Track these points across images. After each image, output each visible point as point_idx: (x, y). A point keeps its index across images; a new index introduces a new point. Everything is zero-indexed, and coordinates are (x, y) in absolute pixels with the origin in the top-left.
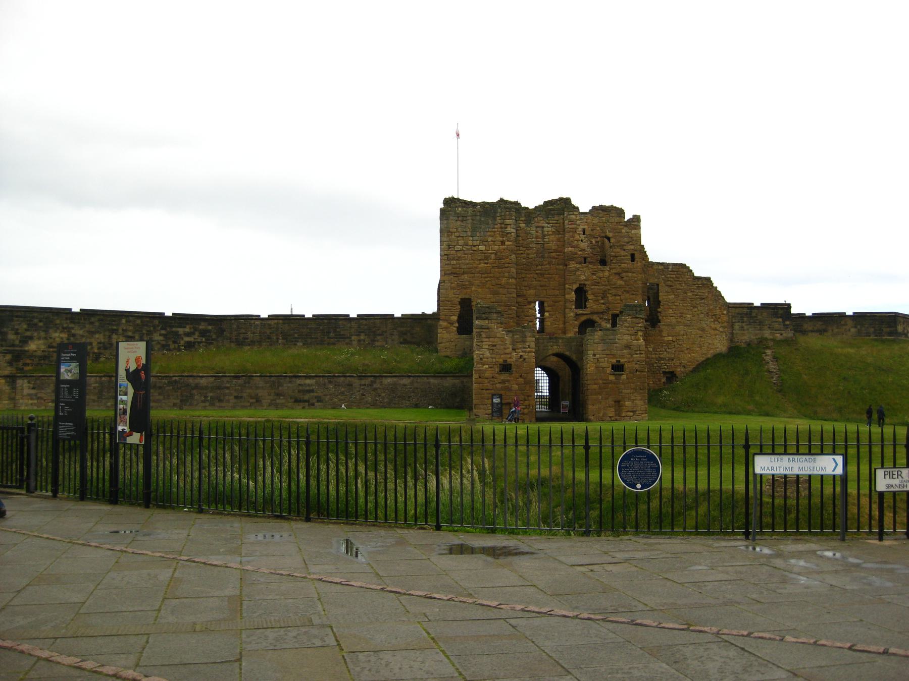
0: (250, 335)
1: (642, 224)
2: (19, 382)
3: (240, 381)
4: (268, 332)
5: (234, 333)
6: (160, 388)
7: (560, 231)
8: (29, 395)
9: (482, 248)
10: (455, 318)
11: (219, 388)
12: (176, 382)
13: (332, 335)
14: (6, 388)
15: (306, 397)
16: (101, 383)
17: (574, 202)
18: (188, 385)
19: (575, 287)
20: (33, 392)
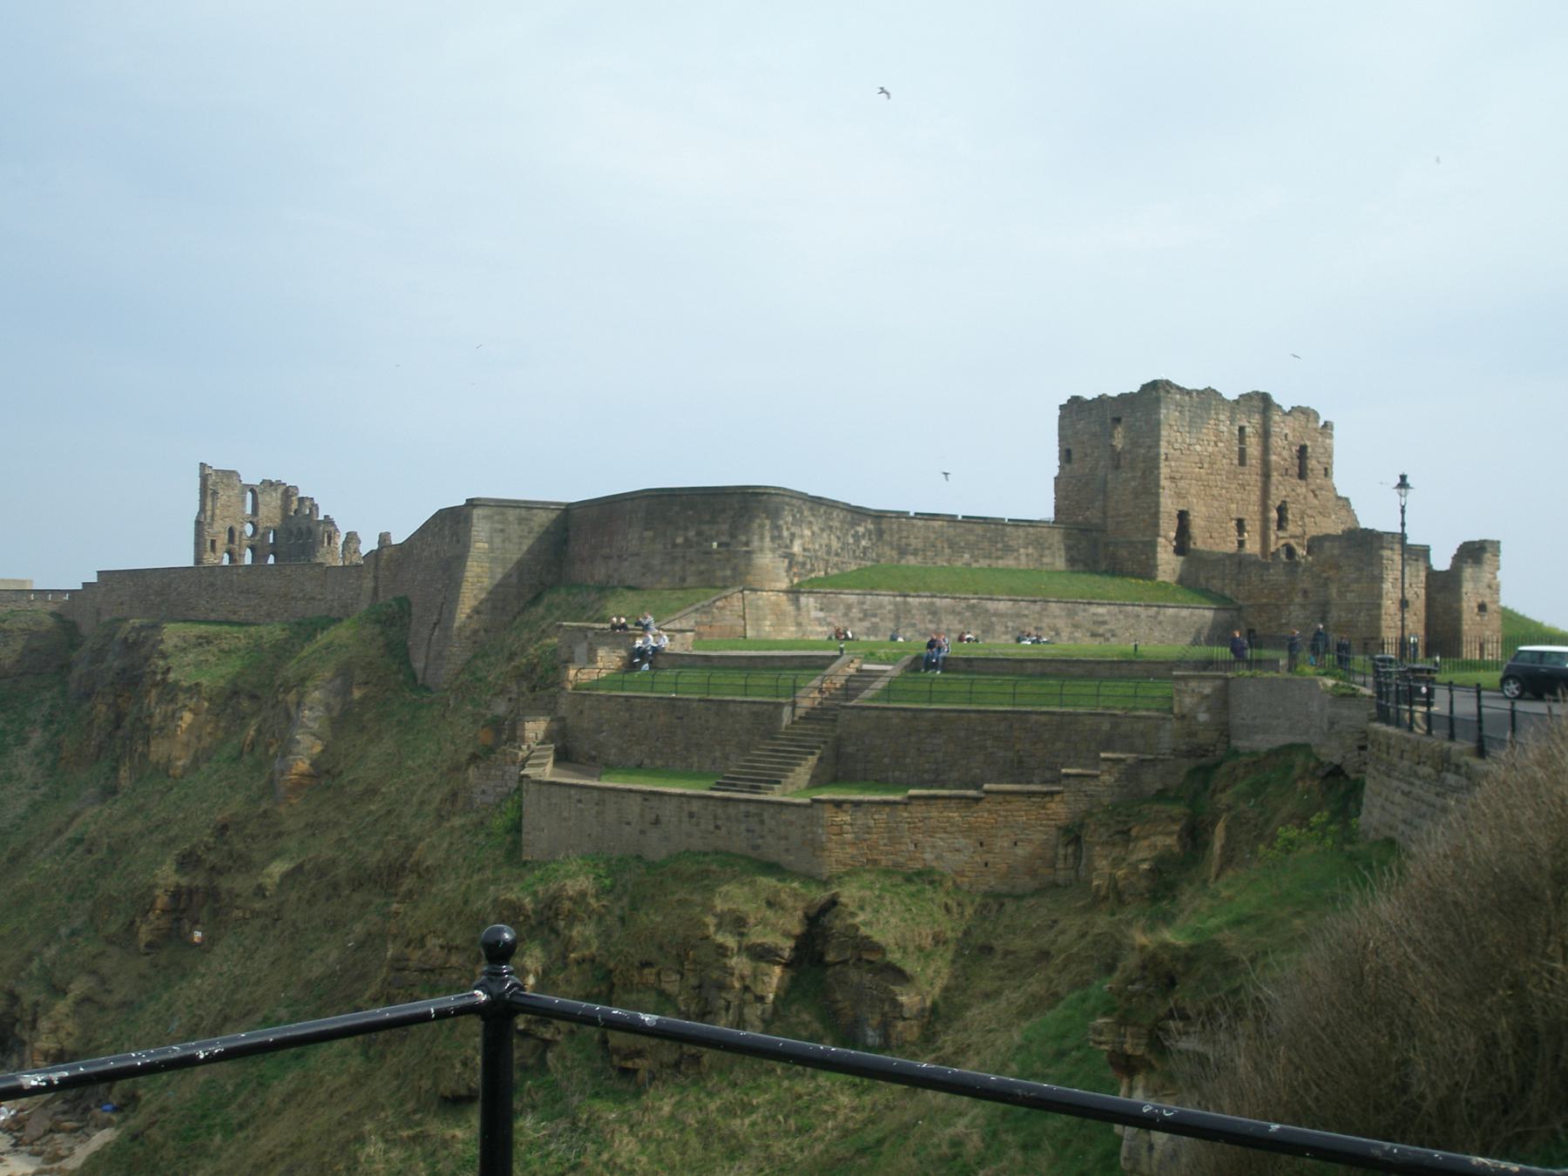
0: (913, 541)
1: (1335, 433)
2: (803, 599)
3: (1037, 607)
4: (933, 536)
5: (896, 537)
6: (959, 613)
7: (1265, 435)
8: (818, 619)
9: (1198, 448)
10: (1173, 535)
11: (1018, 615)
12: (974, 606)
13: (1000, 546)
14: (790, 609)
15: (1101, 631)
16: (896, 604)
17: (1276, 399)
18: (987, 611)
19: (1278, 503)
20: (821, 614)
